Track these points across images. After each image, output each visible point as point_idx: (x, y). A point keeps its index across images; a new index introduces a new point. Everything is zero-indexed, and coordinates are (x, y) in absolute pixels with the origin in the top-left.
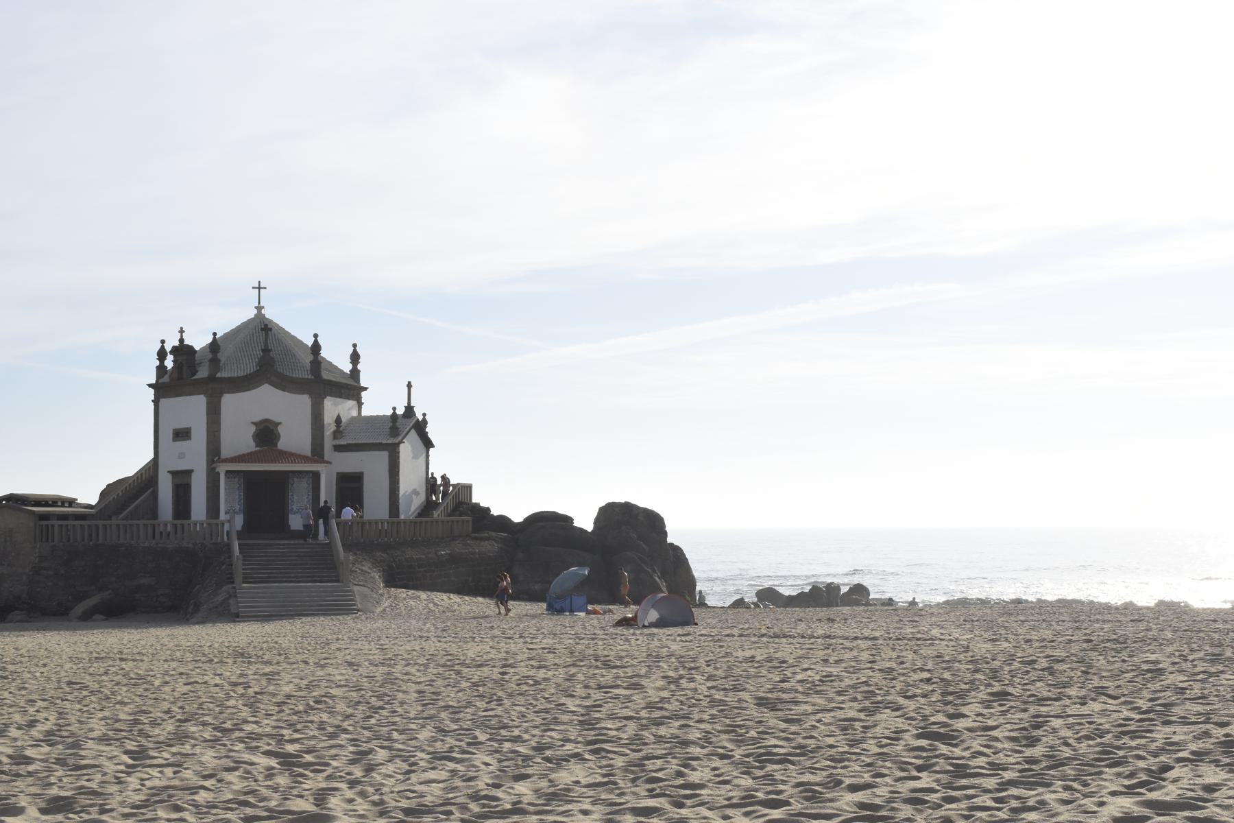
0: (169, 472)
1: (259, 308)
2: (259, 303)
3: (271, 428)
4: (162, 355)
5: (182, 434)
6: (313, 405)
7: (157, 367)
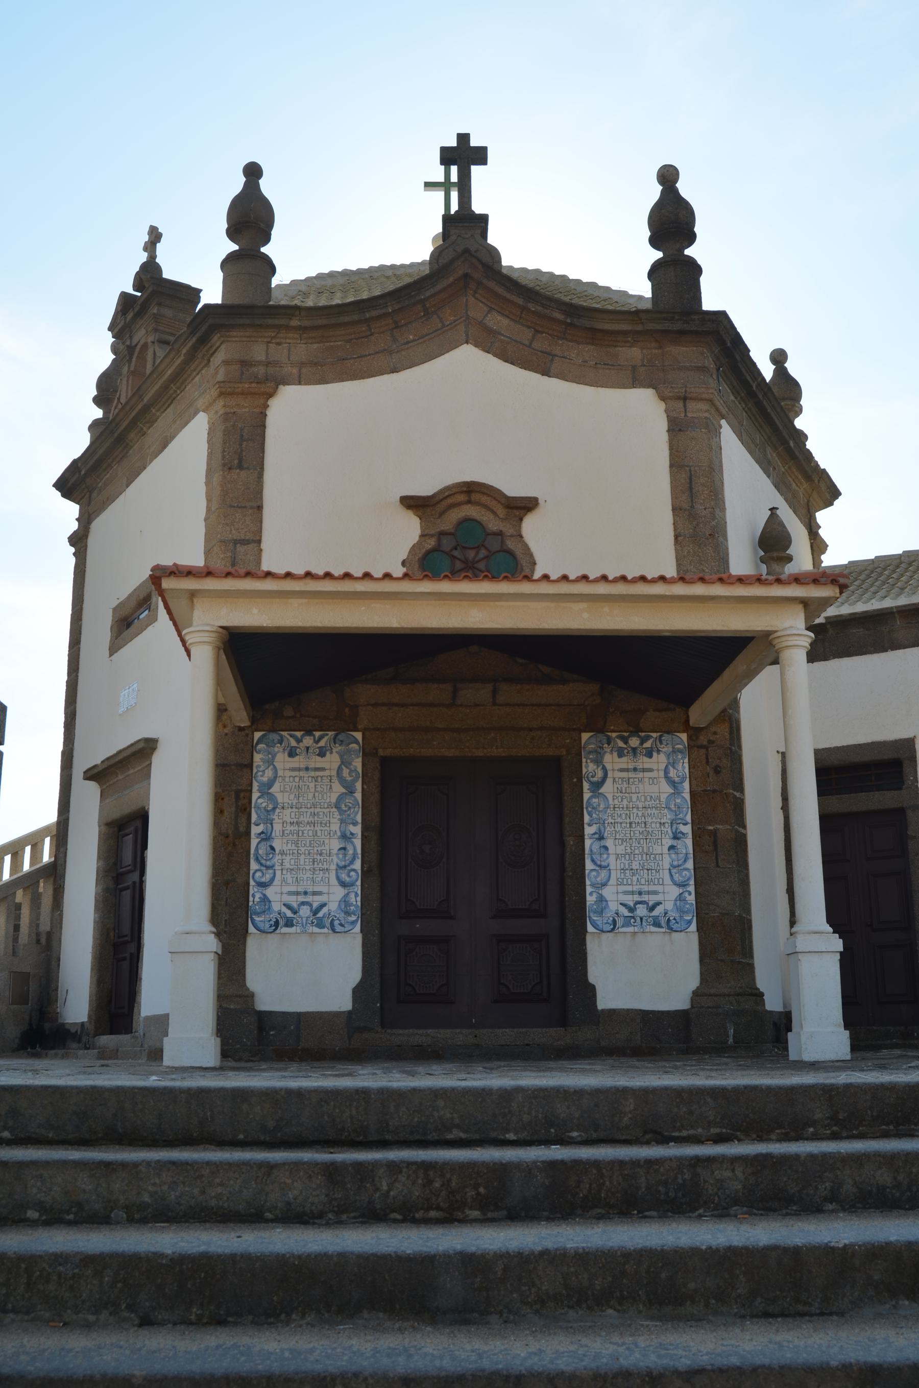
3: (493, 525)
6: (676, 428)
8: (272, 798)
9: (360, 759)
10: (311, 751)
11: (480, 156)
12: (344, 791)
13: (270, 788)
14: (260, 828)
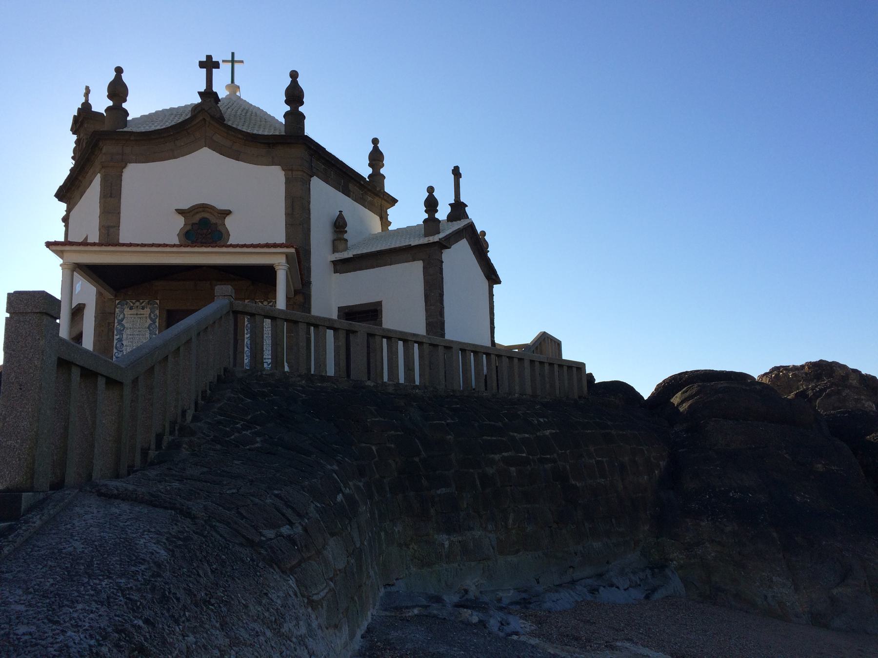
3: (213, 220)
8: (123, 325)
9: (158, 311)
10: (138, 307)
12: (151, 322)
13: (122, 321)
14: (118, 337)
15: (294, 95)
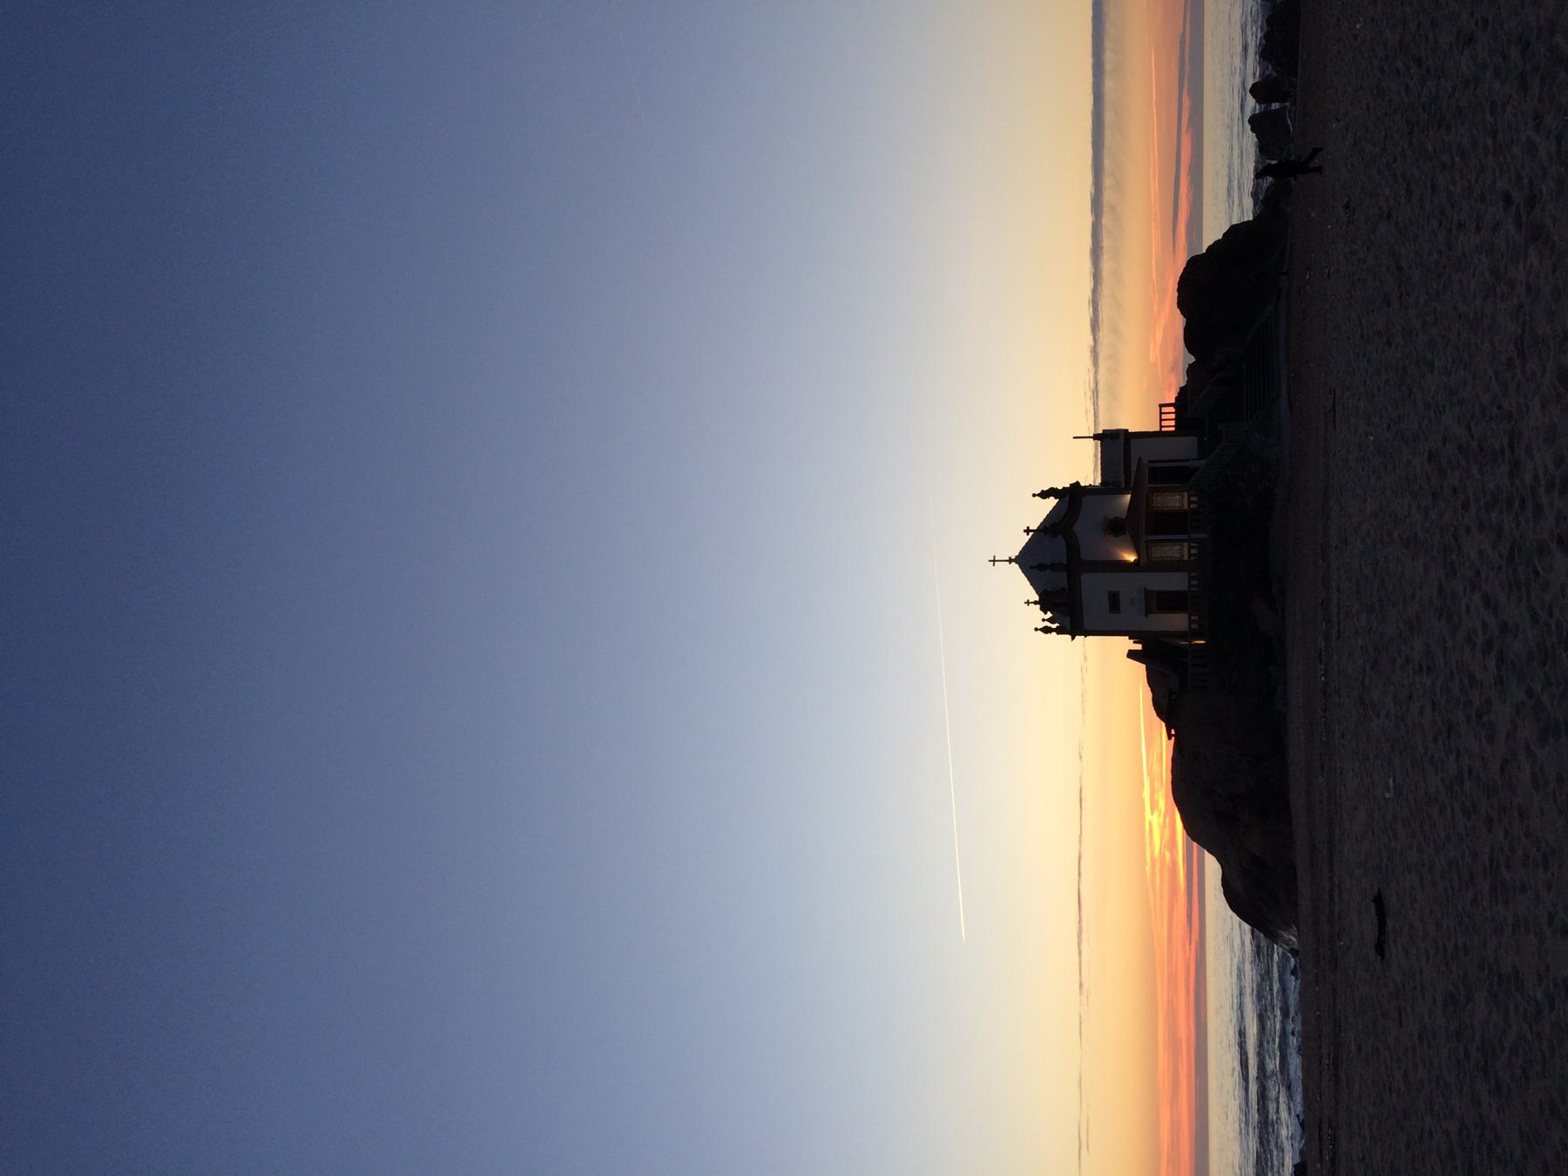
0: (1146, 616)
1: (1010, 561)
2: (1006, 561)
4: (1046, 630)
5: (1114, 602)
7: (1058, 634)
11: (1028, 528)
15: (1044, 495)
